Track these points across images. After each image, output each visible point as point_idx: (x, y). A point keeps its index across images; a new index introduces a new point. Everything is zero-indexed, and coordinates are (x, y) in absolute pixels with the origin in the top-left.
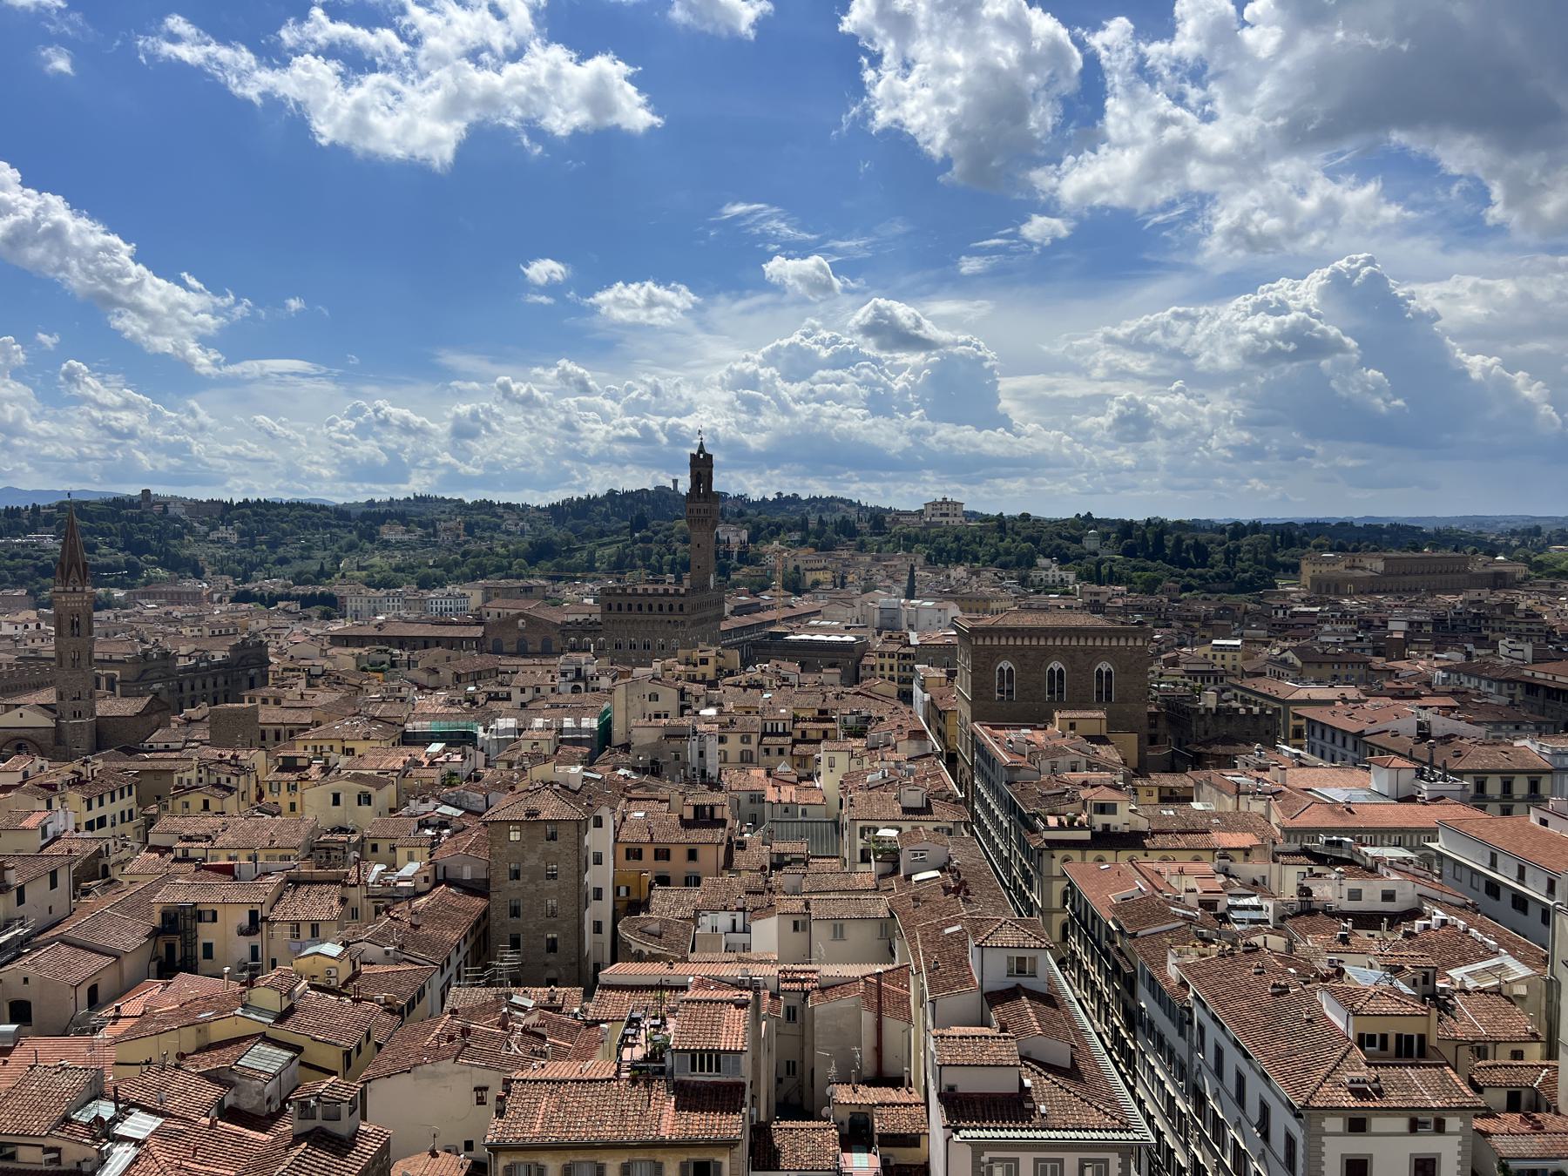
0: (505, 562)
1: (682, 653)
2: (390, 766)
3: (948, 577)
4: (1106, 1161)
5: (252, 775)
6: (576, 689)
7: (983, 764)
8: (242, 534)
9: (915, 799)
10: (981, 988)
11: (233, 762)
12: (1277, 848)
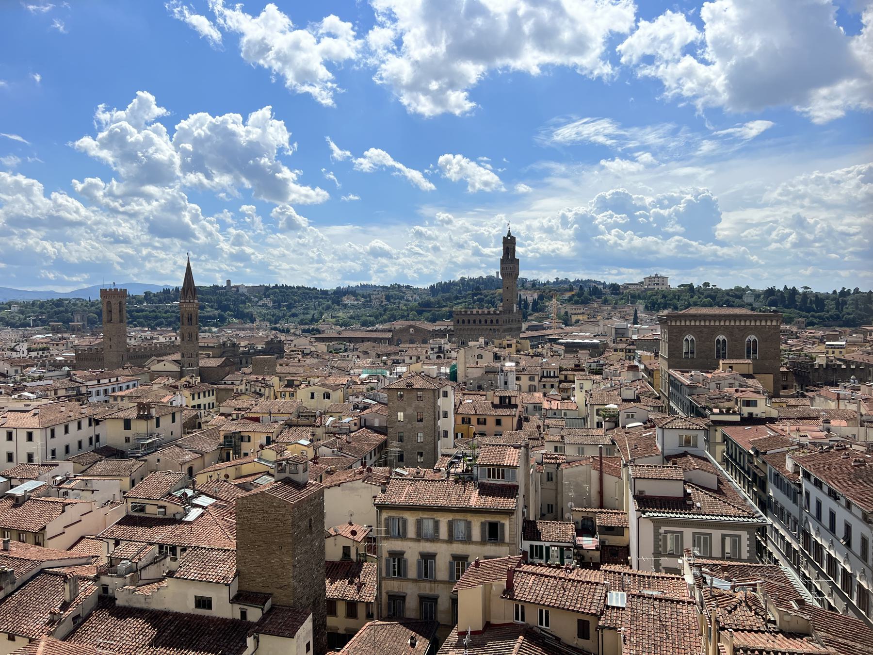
0: (406, 314)
1: (497, 342)
2: (341, 382)
4: (739, 536)
5: (272, 388)
6: (439, 357)
7: (675, 392)
8: (274, 302)
9: (629, 394)
10: (663, 453)
11: (263, 381)
12: (864, 418)
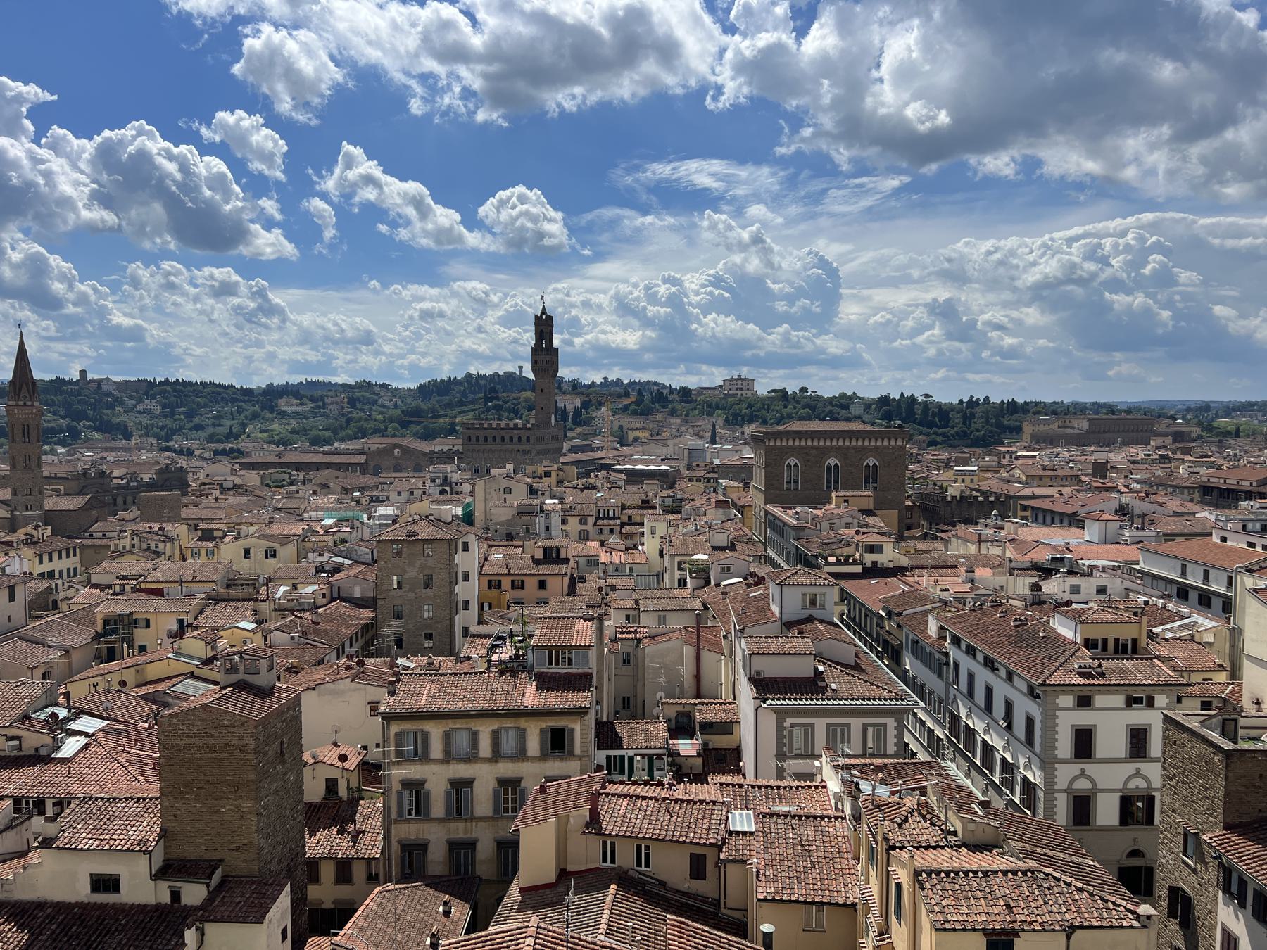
0: (382, 426)
1: (530, 469)
2: (292, 532)
3: (743, 433)
4: (885, 725)
5: (176, 543)
6: (443, 492)
7: (774, 535)
8: (164, 406)
9: (721, 540)
10: (781, 618)
11: (160, 532)
12: (1013, 565)
